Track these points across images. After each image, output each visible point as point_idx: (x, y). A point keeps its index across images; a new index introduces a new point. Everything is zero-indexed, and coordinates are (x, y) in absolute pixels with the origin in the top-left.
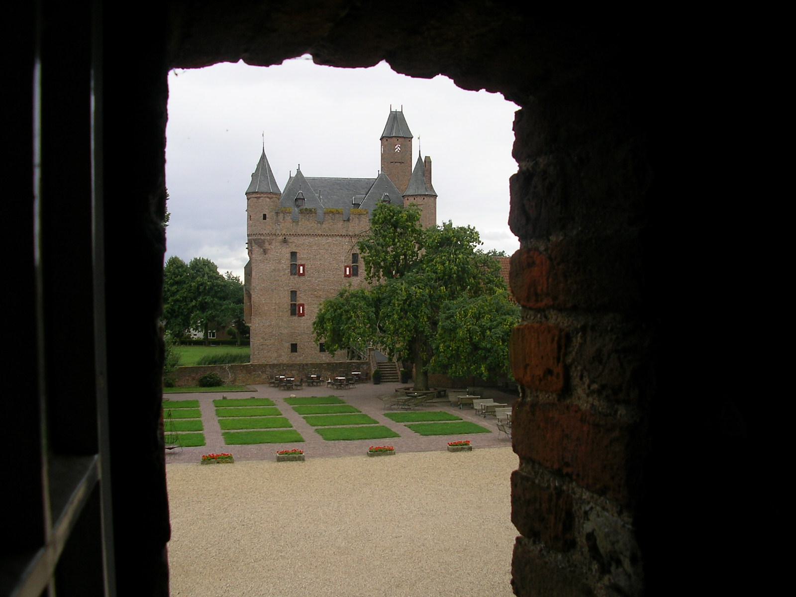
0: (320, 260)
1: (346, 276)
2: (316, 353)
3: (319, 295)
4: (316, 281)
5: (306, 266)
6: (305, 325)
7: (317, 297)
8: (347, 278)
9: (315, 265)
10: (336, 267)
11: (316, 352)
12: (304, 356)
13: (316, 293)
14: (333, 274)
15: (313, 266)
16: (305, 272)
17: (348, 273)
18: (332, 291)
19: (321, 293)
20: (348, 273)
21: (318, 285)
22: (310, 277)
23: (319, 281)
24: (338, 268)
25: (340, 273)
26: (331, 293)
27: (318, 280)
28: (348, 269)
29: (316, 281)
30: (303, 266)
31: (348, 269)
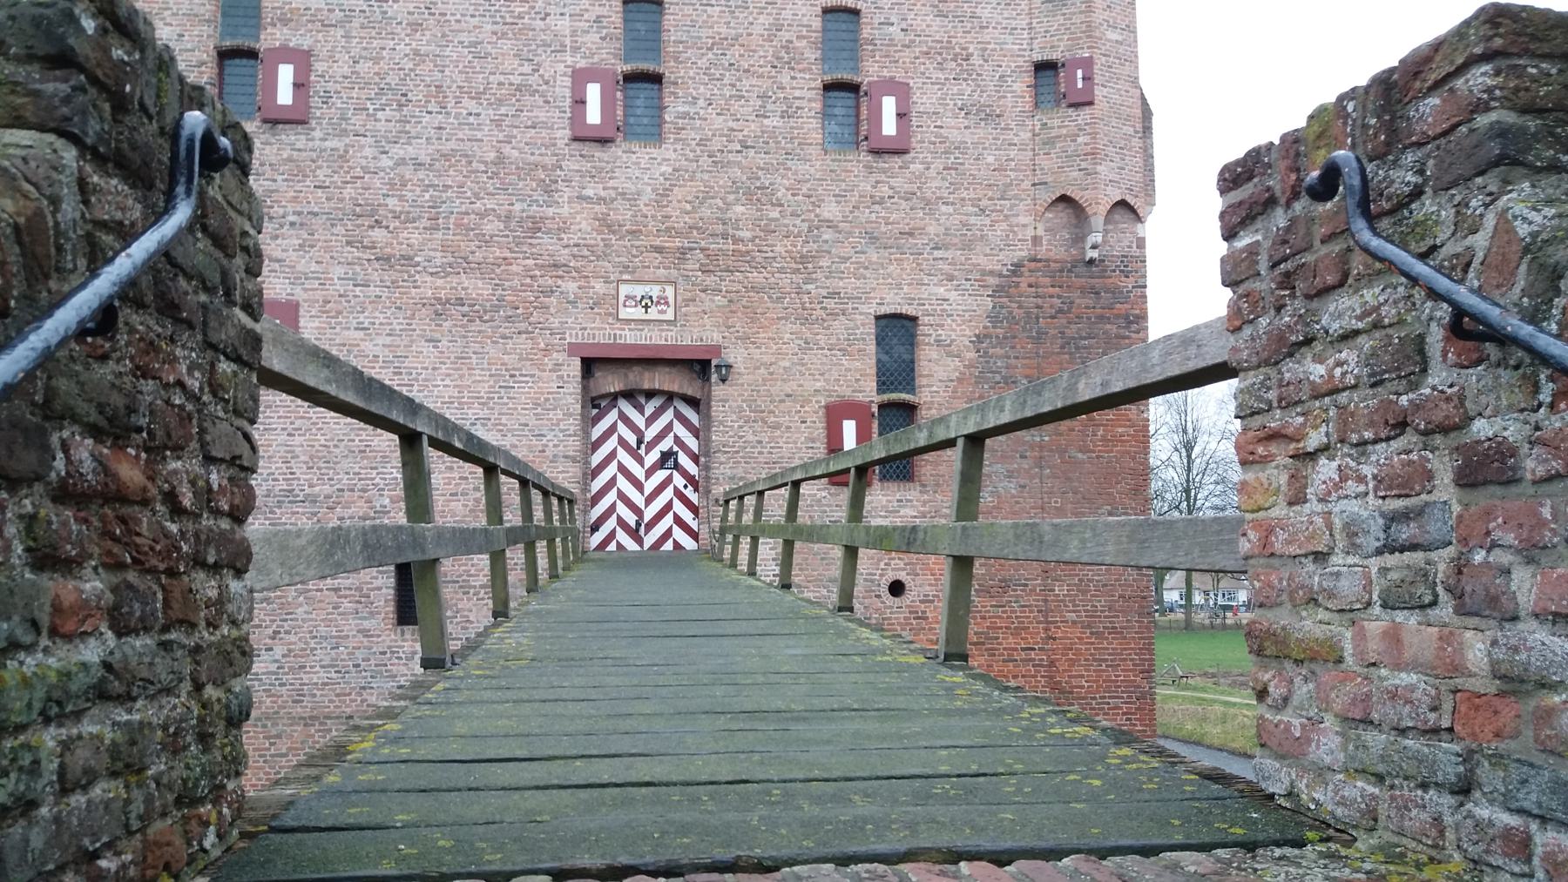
0: (416, 27)
1: (584, 137)
2: (365, 633)
3: (397, 250)
4: (386, 162)
5: (319, 67)
6: (298, 440)
7: (385, 259)
8: (598, 152)
9: (376, 60)
10: (517, 80)
11: (366, 624)
12: (279, 651)
13: (378, 234)
14: (498, 123)
15: (364, 67)
16: (315, 101)
17: (593, 115)
18: (491, 226)
19: (416, 238)
20: (593, 115)
21: (397, 186)
22: (344, 133)
23: (401, 162)
24: (533, 80)
25: (542, 115)
26: (487, 241)
27: (397, 151)
28: (593, 92)
29: (386, 162)
30: (302, 60)
31: (593, 92)
